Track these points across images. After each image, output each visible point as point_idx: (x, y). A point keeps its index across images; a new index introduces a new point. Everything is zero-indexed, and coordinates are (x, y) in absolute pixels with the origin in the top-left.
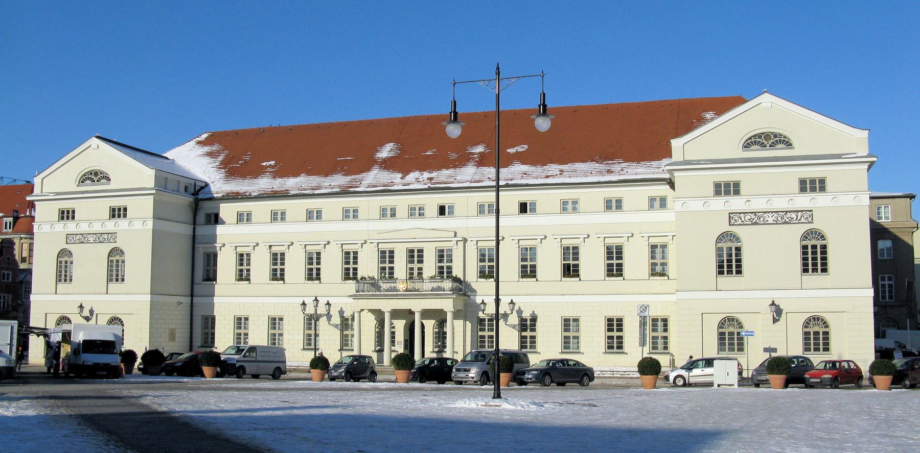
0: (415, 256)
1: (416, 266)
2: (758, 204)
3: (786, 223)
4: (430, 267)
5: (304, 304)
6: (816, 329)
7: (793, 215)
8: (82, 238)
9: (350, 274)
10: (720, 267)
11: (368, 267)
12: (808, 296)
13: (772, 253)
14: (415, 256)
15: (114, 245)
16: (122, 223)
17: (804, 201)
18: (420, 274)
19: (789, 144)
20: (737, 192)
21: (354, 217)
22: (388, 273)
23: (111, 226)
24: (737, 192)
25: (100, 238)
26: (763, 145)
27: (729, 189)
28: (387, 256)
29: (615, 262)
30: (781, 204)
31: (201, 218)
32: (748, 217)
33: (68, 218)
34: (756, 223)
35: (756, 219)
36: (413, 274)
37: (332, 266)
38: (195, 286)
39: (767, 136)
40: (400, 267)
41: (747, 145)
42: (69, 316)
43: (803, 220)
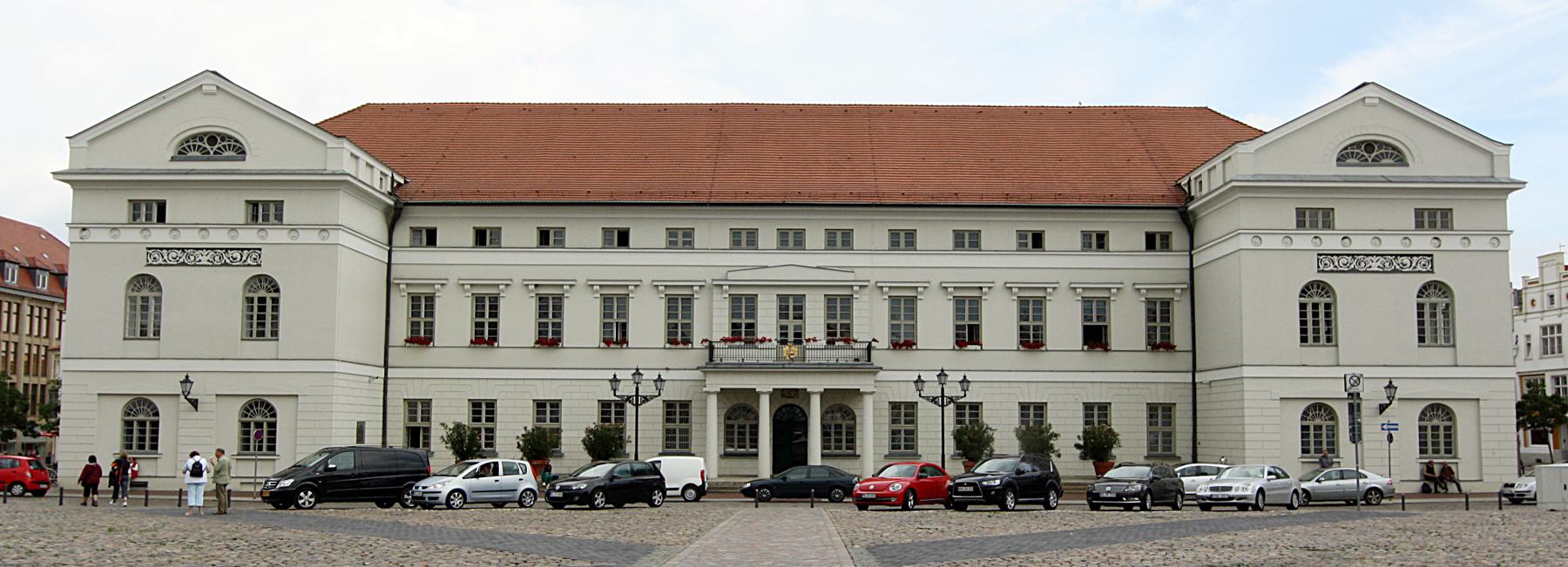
0: (791, 307)
1: (791, 323)
2: (1360, 244)
3: (1395, 271)
4: (815, 324)
5: (615, 380)
6: (1435, 422)
7: (1406, 260)
8: (185, 256)
9: (678, 336)
10: (1303, 331)
11: (712, 320)
12: (1429, 376)
13: (1375, 313)
14: (791, 307)
15: (258, 271)
16: (276, 235)
17: (1422, 242)
18: (798, 335)
19: (1399, 159)
20: (1328, 225)
21: (684, 243)
22: (743, 333)
23: (249, 237)
24: (1328, 225)
25: (223, 257)
26: (1364, 162)
27: (1313, 219)
28: (743, 304)
29: (1031, 323)
30: (1392, 244)
31: (403, 235)
32: (1343, 260)
33: (148, 218)
34: (1354, 271)
35: (1355, 263)
36: (786, 335)
37: (647, 319)
38: (391, 350)
39: (1369, 146)
40: (767, 323)
41: (1342, 159)
42: (272, 401)
43: (1419, 268)
